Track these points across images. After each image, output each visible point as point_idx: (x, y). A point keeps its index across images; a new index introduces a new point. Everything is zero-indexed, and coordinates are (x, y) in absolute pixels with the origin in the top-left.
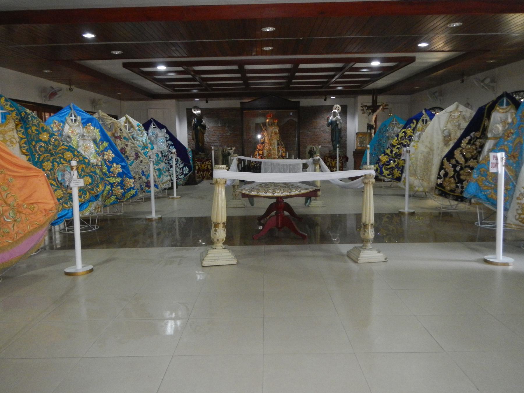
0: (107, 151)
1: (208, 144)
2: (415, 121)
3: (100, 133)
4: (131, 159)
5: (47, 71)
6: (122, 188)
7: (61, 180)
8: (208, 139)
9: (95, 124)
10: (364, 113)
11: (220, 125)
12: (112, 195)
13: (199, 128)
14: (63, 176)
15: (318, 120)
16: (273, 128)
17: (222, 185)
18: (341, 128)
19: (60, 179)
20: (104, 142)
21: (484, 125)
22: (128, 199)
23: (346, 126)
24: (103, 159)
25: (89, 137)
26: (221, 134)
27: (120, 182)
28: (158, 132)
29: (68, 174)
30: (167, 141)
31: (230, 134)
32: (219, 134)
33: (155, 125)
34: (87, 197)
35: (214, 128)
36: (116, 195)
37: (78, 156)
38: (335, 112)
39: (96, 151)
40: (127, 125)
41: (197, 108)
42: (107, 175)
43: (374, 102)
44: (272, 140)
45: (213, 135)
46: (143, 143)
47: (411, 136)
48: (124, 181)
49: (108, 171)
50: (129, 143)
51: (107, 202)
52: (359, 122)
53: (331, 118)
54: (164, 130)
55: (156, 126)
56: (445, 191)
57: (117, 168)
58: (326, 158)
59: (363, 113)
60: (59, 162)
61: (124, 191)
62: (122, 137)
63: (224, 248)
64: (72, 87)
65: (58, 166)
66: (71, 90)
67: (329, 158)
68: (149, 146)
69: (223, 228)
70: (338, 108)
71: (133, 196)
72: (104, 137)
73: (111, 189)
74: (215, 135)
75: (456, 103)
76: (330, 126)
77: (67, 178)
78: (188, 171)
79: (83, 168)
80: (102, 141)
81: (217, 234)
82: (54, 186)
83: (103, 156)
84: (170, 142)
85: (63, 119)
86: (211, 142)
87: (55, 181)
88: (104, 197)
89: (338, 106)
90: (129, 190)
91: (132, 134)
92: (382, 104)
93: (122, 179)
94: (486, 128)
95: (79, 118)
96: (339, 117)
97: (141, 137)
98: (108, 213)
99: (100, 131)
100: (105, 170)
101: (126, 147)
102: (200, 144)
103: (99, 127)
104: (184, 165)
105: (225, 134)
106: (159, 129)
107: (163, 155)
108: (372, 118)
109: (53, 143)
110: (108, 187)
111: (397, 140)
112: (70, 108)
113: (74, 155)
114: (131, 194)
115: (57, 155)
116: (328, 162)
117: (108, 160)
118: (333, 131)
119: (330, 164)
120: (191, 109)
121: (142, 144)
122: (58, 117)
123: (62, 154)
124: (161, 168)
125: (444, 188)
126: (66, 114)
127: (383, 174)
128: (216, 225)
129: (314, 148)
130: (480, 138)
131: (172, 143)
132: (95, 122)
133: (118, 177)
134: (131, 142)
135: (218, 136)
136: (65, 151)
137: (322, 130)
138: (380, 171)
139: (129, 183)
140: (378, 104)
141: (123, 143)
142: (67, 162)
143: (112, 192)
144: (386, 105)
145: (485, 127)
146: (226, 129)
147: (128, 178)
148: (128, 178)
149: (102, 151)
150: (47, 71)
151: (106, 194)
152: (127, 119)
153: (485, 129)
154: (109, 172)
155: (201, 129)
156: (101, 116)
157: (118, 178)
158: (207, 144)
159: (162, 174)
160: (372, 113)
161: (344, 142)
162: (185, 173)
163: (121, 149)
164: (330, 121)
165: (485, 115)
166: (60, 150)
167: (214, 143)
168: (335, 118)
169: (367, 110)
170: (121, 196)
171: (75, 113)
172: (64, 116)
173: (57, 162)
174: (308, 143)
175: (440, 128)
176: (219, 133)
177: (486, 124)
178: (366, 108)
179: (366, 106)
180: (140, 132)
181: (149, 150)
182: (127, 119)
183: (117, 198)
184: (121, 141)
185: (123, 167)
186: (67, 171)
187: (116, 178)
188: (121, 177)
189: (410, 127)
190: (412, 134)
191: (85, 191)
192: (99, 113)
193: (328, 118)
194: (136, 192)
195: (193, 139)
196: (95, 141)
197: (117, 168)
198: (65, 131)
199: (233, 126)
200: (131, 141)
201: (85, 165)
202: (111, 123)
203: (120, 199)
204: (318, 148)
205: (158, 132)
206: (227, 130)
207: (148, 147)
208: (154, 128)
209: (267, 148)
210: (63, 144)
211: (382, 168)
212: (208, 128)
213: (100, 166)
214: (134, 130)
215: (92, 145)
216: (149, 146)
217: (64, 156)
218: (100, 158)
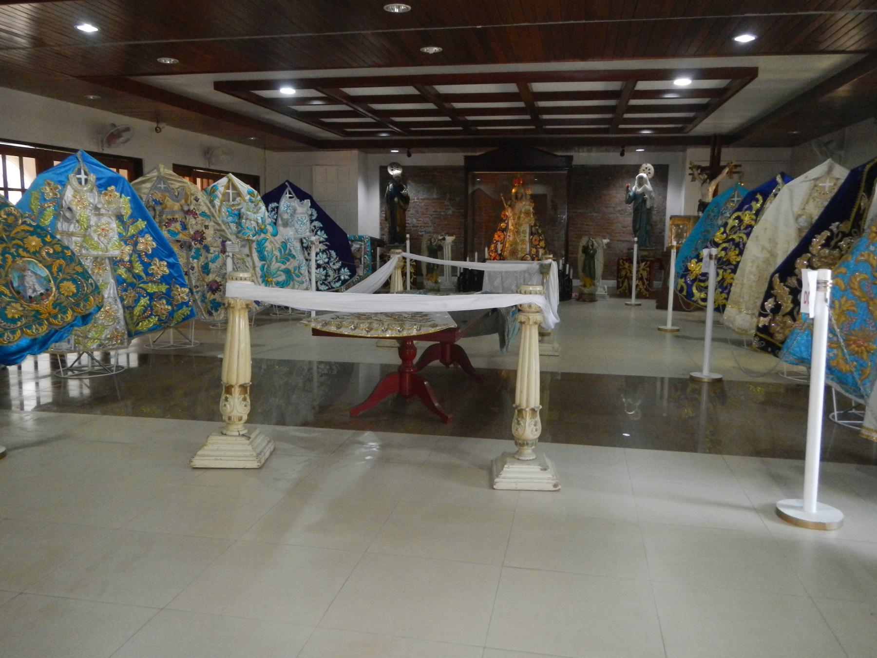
0: (143, 237)
1: (414, 229)
2: (759, 197)
3: (131, 203)
4: (214, 251)
5: (91, 97)
6: (169, 303)
7: (19, 286)
8: (415, 220)
9: (123, 189)
10: (694, 179)
11: (435, 196)
12: (151, 314)
13: (396, 199)
14: (22, 278)
15: (613, 192)
16: (524, 203)
17: (239, 310)
18: (651, 207)
19: (16, 284)
20: (138, 220)
21: (860, 205)
22: (178, 323)
23: (666, 204)
24: (133, 251)
25: (109, 211)
26: (437, 212)
27: (164, 291)
28: (297, 205)
29: (31, 276)
30: (312, 221)
31: (453, 212)
33: (292, 193)
34: (67, 317)
35: (426, 201)
36: (159, 315)
37: (53, 243)
38: (641, 178)
39: (120, 234)
40: (230, 191)
41: (395, 165)
42: (143, 278)
43: (715, 158)
44: (521, 225)
45: (424, 214)
46: (257, 223)
47: (750, 227)
48: (173, 290)
49: (144, 273)
50: (212, 224)
51: (142, 326)
52: (686, 194)
53: (634, 189)
54: (307, 202)
55: (294, 195)
56: (774, 342)
57: (160, 268)
58: (621, 261)
59: (692, 181)
60: (15, 254)
61: (173, 308)
62: (197, 212)
63: (243, 435)
64: (161, 126)
65: (13, 262)
66: (158, 130)
67: (627, 261)
68: (270, 228)
69: (240, 394)
70: (649, 170)
71: (186, 318)
72: (139, 211)
73: (150, 303)
74: (426, 214)
75: (829, 161)
76: (632, 204)
77: (29, 284)
78: (349, 276)
79: (61, 265)
80: (134, 218)
81: (228, 406)
82: (6, 295)
83: (136, 244)
84: (317, 224)
85: (62, 178)
86: (419, 225)
87: (9, 288)
88: (135, 318)
89: (649, 166)
90: (180, 306)
91: (240, 207)
92: (728, 164)
93: (168, 287)
94: (863, 214)
95: (92, 177)
96: (649, 186)
97: (254, 213)
98: (172, 343)
99: (130, 201)
100: (138, 269)
101: (204, 231)
102: (398, 229)
103: (130, 194)
104: (342, 264)
105: (444, 212)
106: (299, 200)
107: (304, 245)
108: (708, 190)
109: (5, 219)
110: (144, 301)
111: (722, 233)
112: (78, 159)
113: (45, 243)
114: (184, 315)
115: (11, 243)
116: (624, 268)
117: (145, 252)
118: (636, 210)
119: (627, 273)
120: (386, 168)
121: (254, 224)
122: (55, 174)
123: (22, 240)
124: (291, 268)
125: (772, 335)
126: (69, 170)
127: (693, 299)
128: (229, 389)
129: (595, 243)
130: (849, 235)
131: (321, 225)
132: (123, 185)
133: (161, 283)
134: (214, 222)
136: (27, 234)
137: (619, 211)
138: (687, 292)
139: (179, 294)
140: (722, 164)
141: (200, 222)
142: (30, 254)
143: (152, 310)
144: (736, 166)
145: (861, 212)
146: (446, 203)
147: (179, 285)
148: (178, 286)
149: (133, 236)
150: (91, 97)
151: (140, 311)
152: (230, 180)
153: (861, 216)
154: (147, 274)
155: (400, 202)
156: (162, 174)
157: (162, 284)
159: (293, 280)
160: (708, 180)
161: (660, 233)
162: (342, 278)
163: (194, 233)
164: (631, 194)
165: (863, 184)
166: (18, 232)
167: (424, 227)
168: (641, 188)
169: (699, 174)
170: (166, 317)
171: (86, 167)
172: (63, 172)
173: (12, 254)
174: (592, 233)
175: (793, 212)
176: (433, 210)
177: (862, 204)
178: (699, 171)
179: (699, 167)
180: (253, 205)
181: (269, 236)
182: (230, 180)
183: (159, 320)
184: (195, 218)
185: (170, 265)
186: (29, 270)
187: (158, 285)
188: (167, 284)
189: (750, 209)
190: (753, 223)
191: (65, 307)
192: (159, 171)
193: (628, 187)
194: (192, 311)
195: (386, 220)
196: (119, 217)
197: (160, 268)
198: (66, 197)
199: (457, 199)
200: (215, 220)
201: (64, 260)
202: (178, 188)
203: (164, 323)
204: (600, 242)
205: (297, 205)
206: (448, 206)
207: (267, 230)
208: (290, 198)
209: (511, 239)
210: (24, 223)
211: (692, 285)
212: (416, 200)
213: (127, 262)
214: (242, 201)
215: (114, 224)
216: (270, 228)
217: (24, 243)
218: (128, 249)
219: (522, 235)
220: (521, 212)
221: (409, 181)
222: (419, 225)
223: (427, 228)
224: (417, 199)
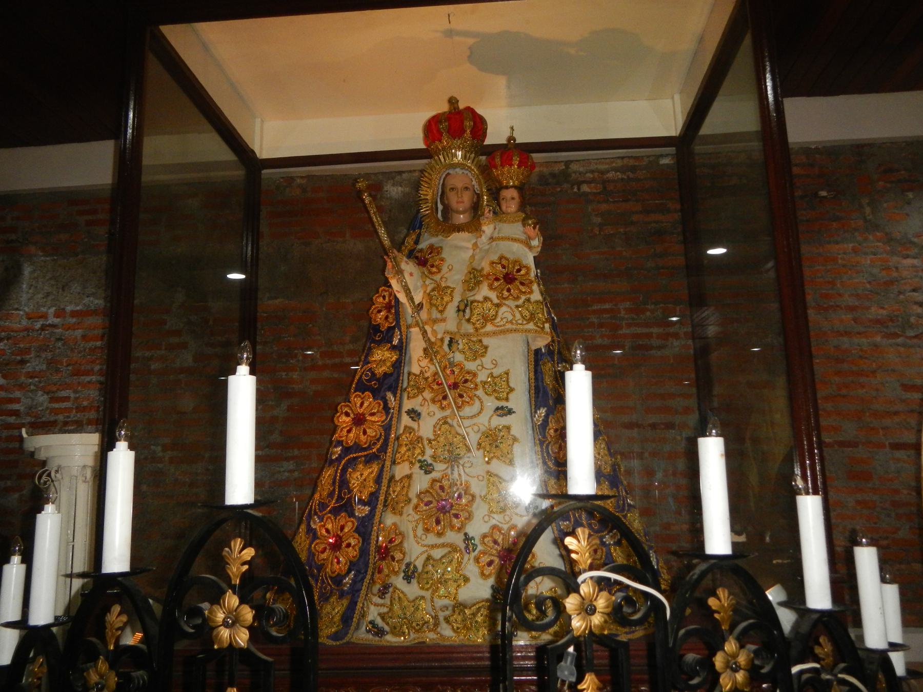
8: (42, 398)
45: (77, 373)
86: (61, 418)
137: (878, 321)
212: (52, 320)
219: (491, 403)
220: (474, 278)
221: (33, 249)
224: (57, 315)
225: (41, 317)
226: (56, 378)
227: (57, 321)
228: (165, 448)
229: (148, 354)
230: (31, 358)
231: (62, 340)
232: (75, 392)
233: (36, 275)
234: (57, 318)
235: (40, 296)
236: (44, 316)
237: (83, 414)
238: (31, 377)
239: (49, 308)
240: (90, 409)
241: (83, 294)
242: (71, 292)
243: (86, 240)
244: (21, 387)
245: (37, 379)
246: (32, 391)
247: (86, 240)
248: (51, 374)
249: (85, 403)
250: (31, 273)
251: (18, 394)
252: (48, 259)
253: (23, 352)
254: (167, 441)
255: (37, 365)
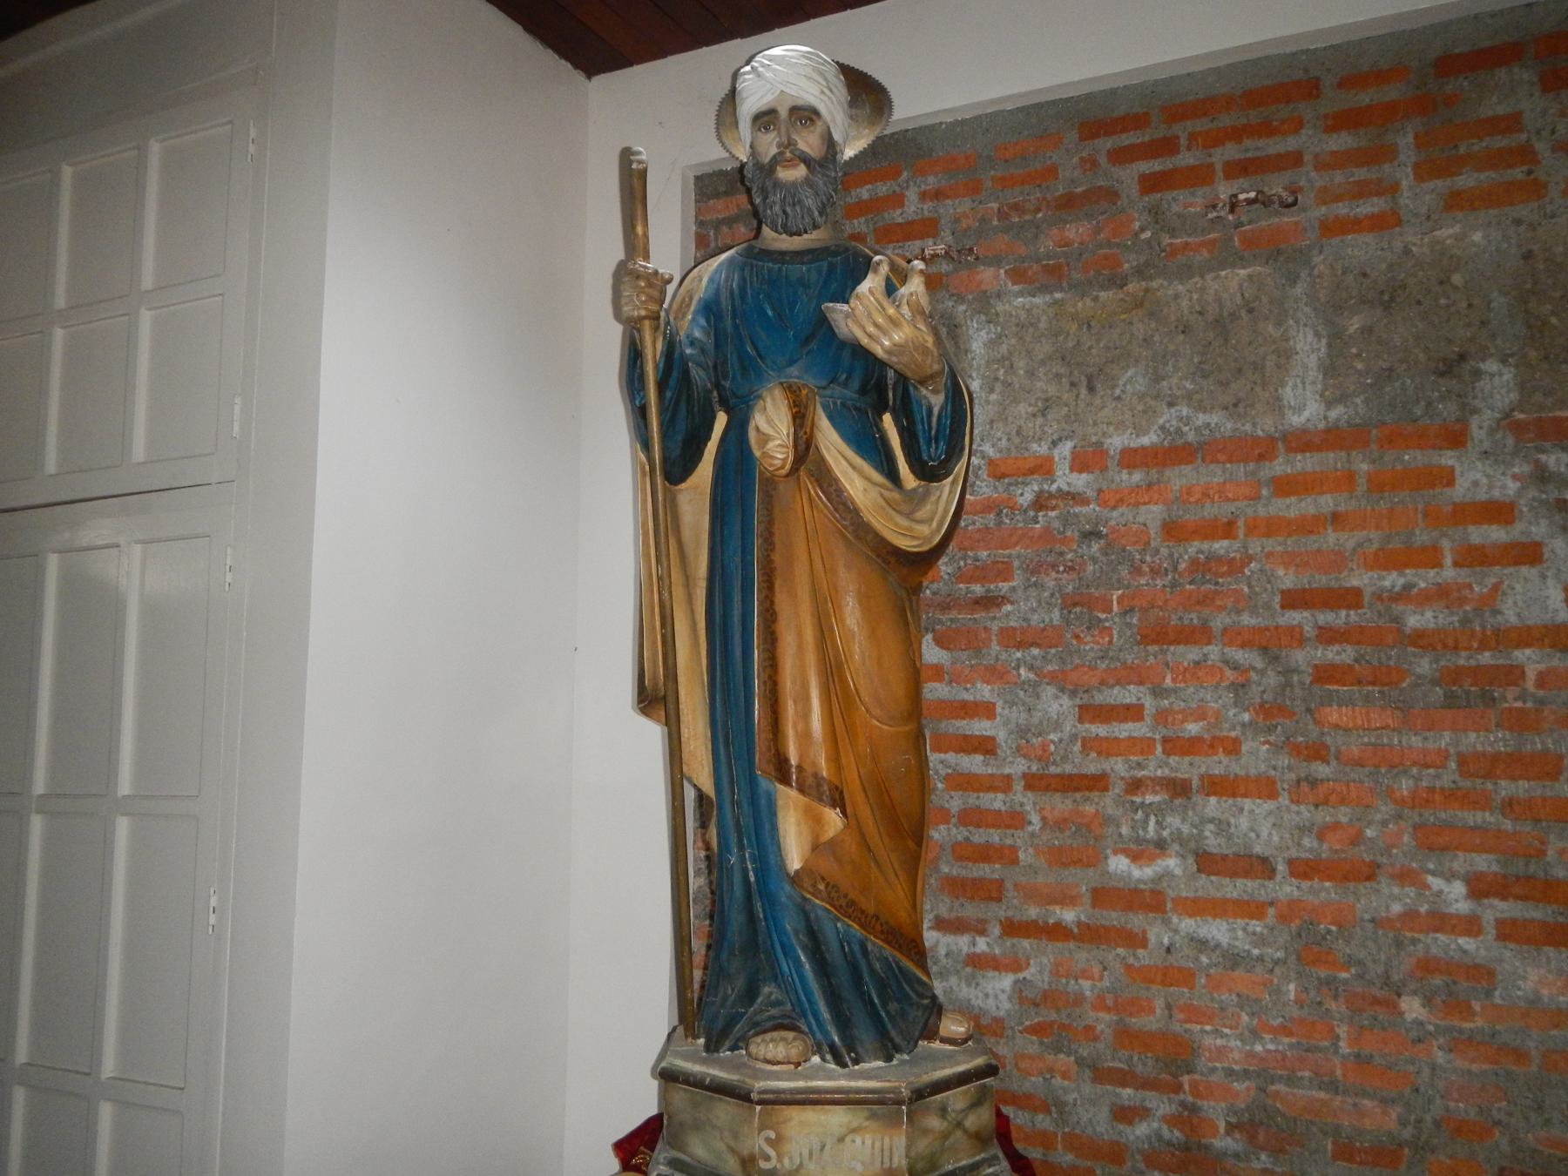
1: (1061, 804)
8: (1056, 705)
26: (1351, 598)
32: (1293, 600)
45: (1158, 635)
135: (1269, 643)
155: (831, 442)
158: (1023, 798)
176: (1288, 579)
206: (1499, 512)
212: (1066, 479)
222: (1118, 767)
223: (1213, 805)
225: (1032, 471)
226: (1091, 646)
227: (1080, 481)
228: (1479, 888)
229: (1392, 580)
230: (1013, 589)
231: (1097, 535)
232: (1158, 692)
233: (1004, 349)
234: (1081, 472)
235: (1023, 409)
236: (1044, 468)
237: (1187, 759)
238: (1020, 645)
239: (1054, 444)
240: (1212, 746)
241: (1156, 397)
242: (1118, 392)
243: (1147, 235)
244: (995, 674)
245: (1035, 651)
246: (1023, 685)
247: (1147, 235)
248: (1077, 637)
249: (1193, 728)
250: (992, 344)
251: (984, 691)
252: (1037, 300)
253: (981, 573)
254: (1484, 863)
255: (1034, 610)
